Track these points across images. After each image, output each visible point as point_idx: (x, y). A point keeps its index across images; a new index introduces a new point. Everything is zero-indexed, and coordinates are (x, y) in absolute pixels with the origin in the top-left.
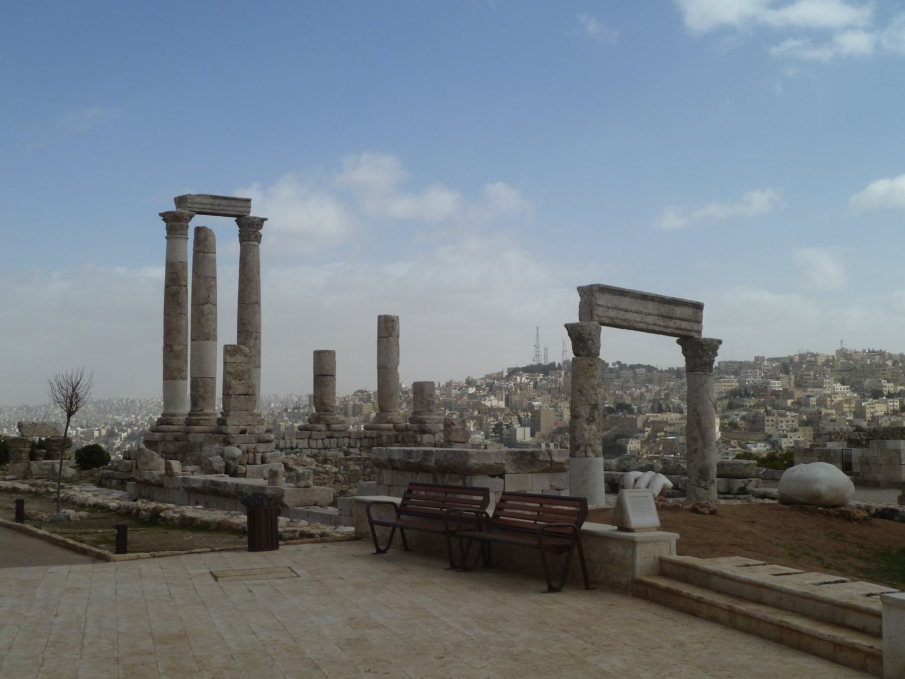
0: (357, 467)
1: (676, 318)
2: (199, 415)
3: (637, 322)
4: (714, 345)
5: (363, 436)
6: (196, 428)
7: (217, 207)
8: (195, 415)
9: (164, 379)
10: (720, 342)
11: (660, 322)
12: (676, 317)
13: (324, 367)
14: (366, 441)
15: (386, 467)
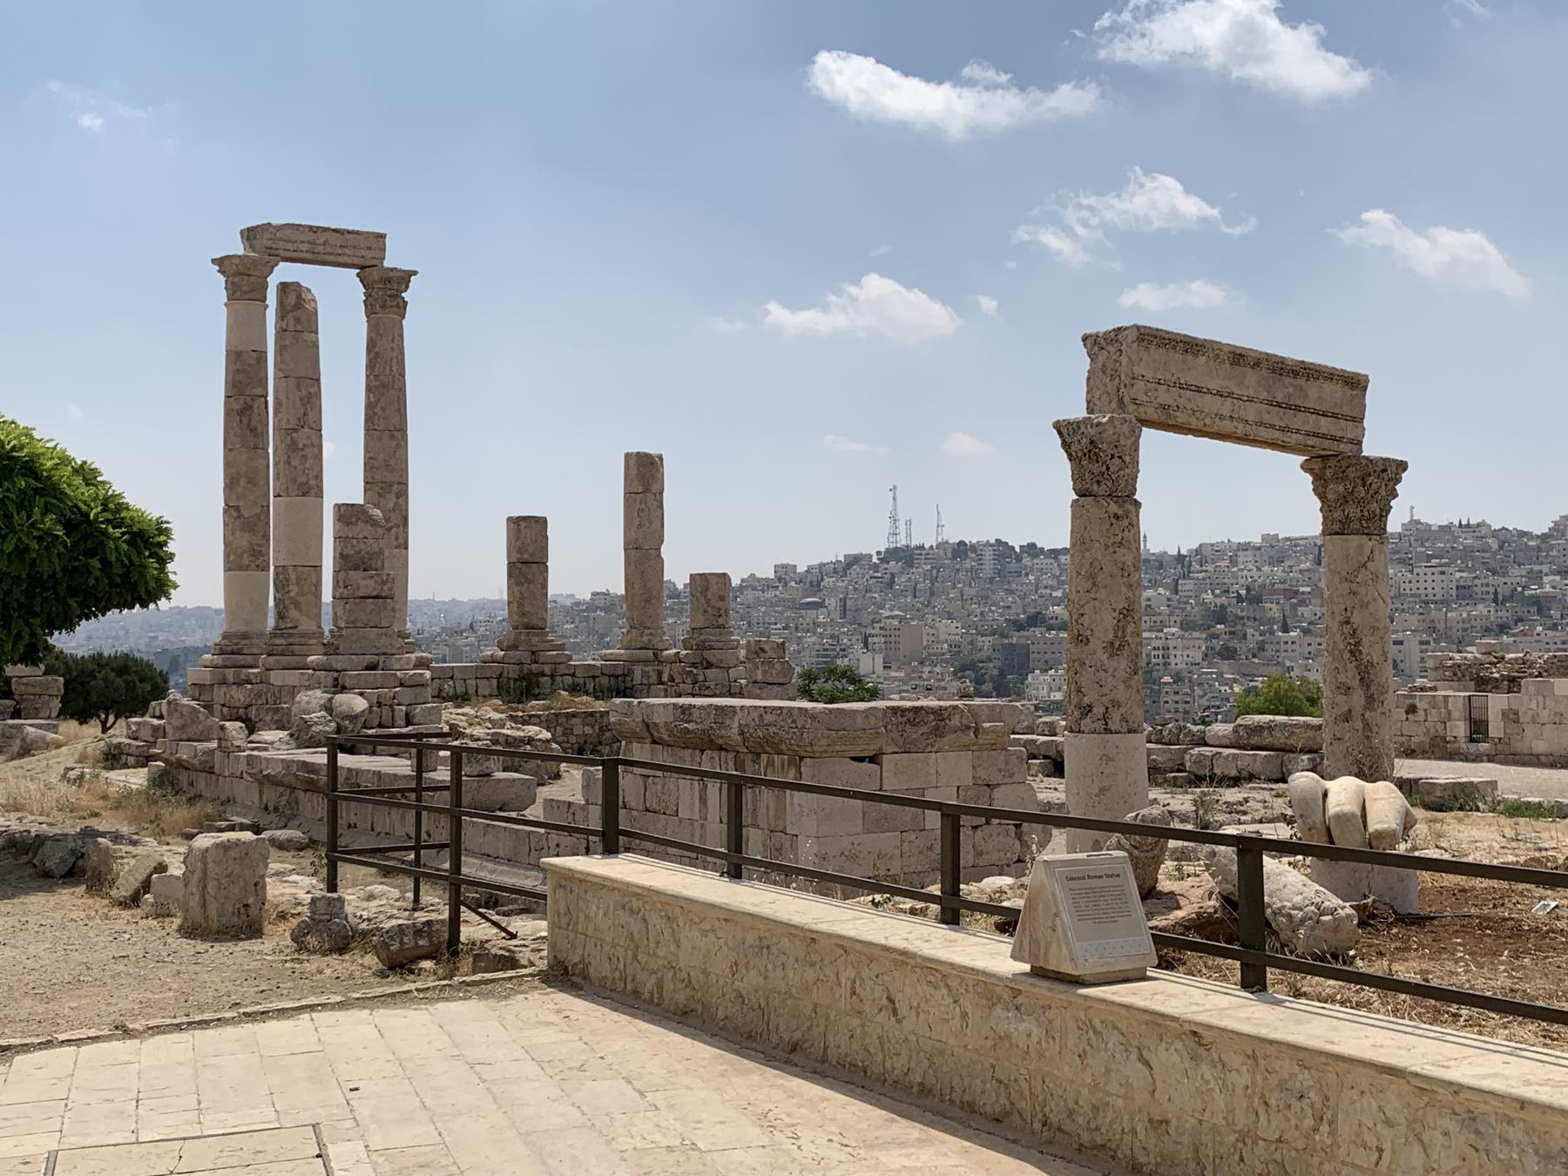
0: (588, 730)
1: (1307, 410)
2: (291, 635)
3: (1221, 417)
4: (1392, 471)
5: (598, 673)
7: (321, 249)
8: (282, 636)
9: (227, 569)
10: (1403, 466)
11: (1274, 417)
12: (1306, 411)
13: (528, 545)
14: (604, 680)
15: (640, 739)
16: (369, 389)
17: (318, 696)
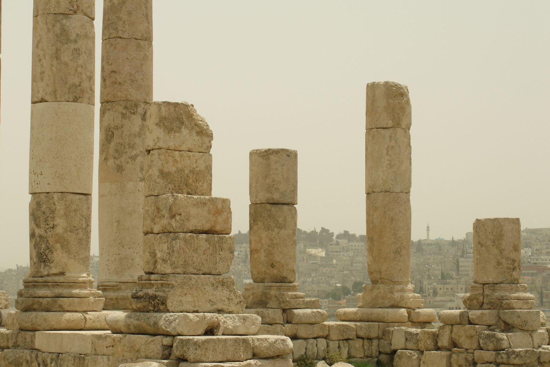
2: (57, 284)
5: (352, 335)
6: (52, 317)
8: (46, 284)
14: (358, 344)
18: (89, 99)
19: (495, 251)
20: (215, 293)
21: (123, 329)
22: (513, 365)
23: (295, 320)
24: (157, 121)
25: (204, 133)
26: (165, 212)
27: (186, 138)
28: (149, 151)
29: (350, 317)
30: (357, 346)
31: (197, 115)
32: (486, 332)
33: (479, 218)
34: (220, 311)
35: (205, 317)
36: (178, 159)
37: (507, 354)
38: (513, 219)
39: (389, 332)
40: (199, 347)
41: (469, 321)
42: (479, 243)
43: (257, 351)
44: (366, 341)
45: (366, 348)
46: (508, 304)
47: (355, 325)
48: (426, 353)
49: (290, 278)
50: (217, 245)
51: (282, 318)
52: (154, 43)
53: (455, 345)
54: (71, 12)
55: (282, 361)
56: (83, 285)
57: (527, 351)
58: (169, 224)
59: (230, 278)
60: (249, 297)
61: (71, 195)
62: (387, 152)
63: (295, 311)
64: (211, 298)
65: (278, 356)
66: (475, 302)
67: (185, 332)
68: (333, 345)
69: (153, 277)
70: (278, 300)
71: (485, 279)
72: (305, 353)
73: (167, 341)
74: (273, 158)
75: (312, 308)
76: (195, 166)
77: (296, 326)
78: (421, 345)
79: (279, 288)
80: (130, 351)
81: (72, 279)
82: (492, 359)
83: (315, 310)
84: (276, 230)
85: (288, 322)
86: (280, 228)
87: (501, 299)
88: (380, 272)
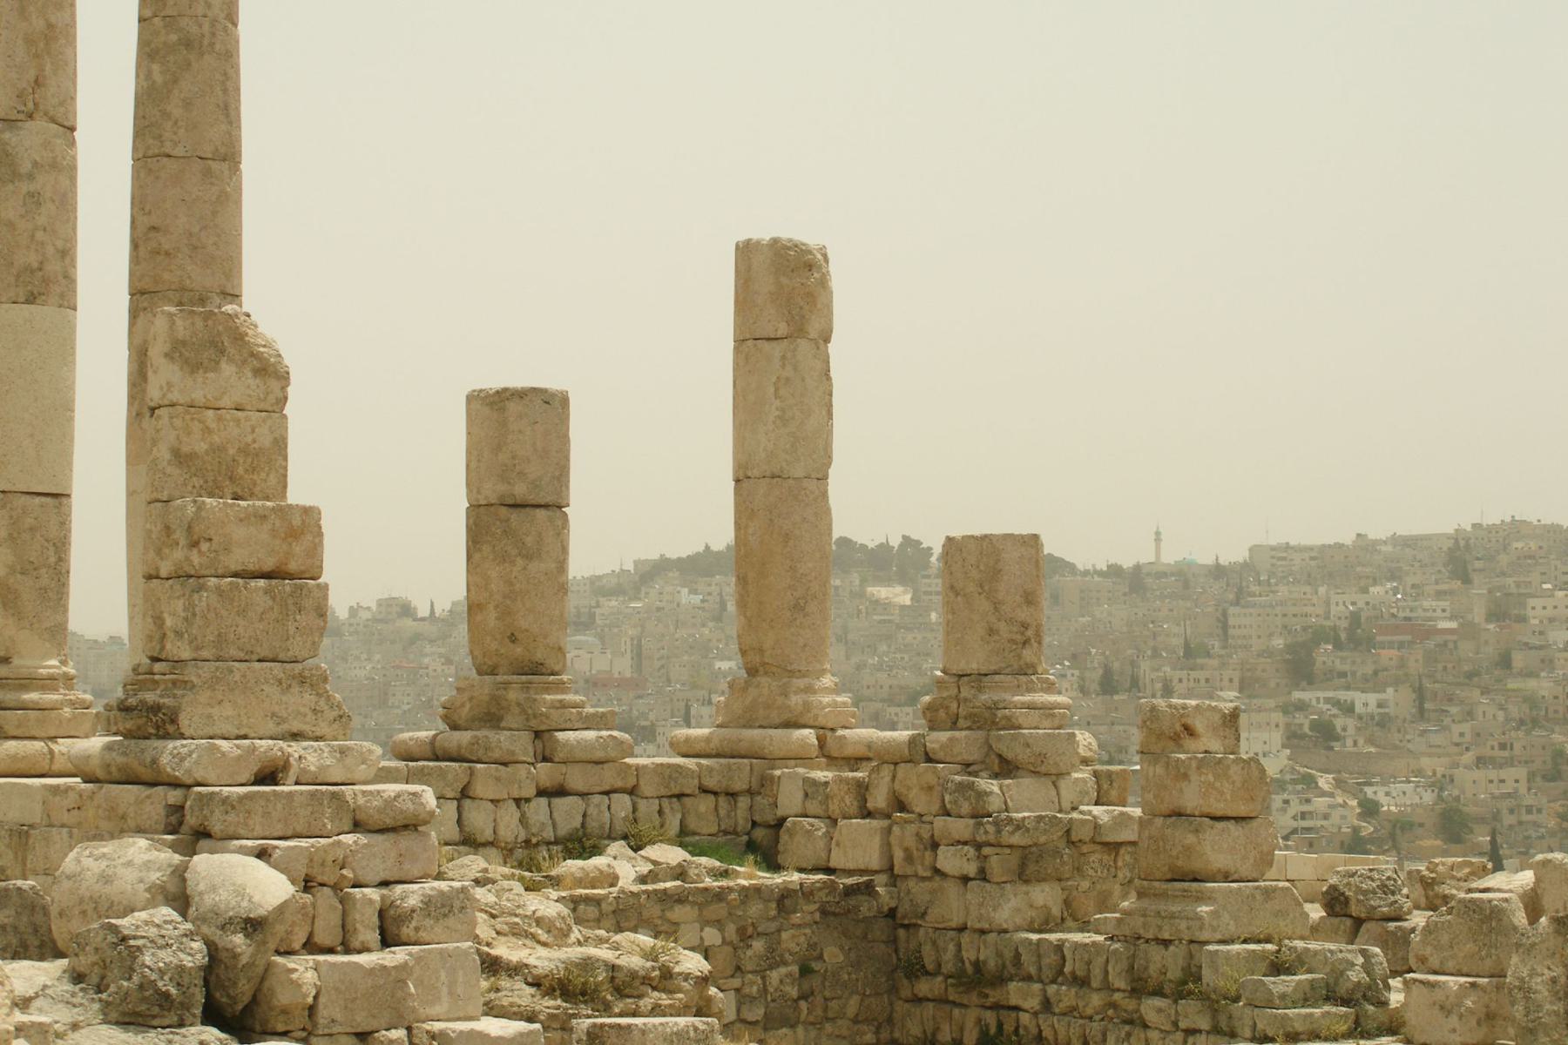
5: (691, 786)
13: (517, 463)
14: (705, 804)
16: (148, 52)
17: (140, 858)
18: (62, 296)
19: (983, 605)
20: (284, 698)
21: (100, 774)
22: (1010, 846)
23: (560, 755)
24: (167, 348)
25: (271, 372)
26: (180, 535)
27: (231, 382)
28: (153, 410)
29: (698, 748)
30: (702, 808)
31: (263, 336)
32: (958, 778)
33: (952, 535)
34: (296, 736)
35: (254, 749)
36: (213, 425)
37: (996, 823)
38: (1022, 536)
39: (772, 777)
40: (233, 807)
41: (926, 754)
42: (952, 587)
43: (361, 816)
44: (722, 799)
45: (722, 812)
46: (1008, 719)
47: (698, 765)
48: (841, 823)
49: (552, 663)
50: (290, 601)
51: (531, 750)
52: (244, 167)
53: (902, 807)
54: (21, 117)
55: (414, 835)
56: (50, 683)
57: (1040, 819)
58: (187, 559)
59: (318, 668)
60: (463, 705)
61: (24, 498)
62: (777, 390)
63: (560, 735)
64: (276, 708)
65: (406, 827)
66: (942, 713)
67: (212, 778)
68: (647, 808)
69: (158, 667)
70: (524, 711)
71: (962, 666)
72: (583, 825)
73: (174, 796)
74: (513, 407)
75: (599, 729)
76: (249, 439)
77: (563, 768)
78: (834, 808)
79: (526, 687)
80: (109, 818)
81: (24, 672)
82: (966, 836)
83: (604, 733)
84: (520, 562)
85: (545, 759)
86: (529, 557)
87: (994, 707)
88: (761, 651)
